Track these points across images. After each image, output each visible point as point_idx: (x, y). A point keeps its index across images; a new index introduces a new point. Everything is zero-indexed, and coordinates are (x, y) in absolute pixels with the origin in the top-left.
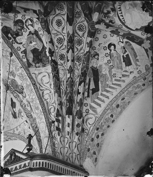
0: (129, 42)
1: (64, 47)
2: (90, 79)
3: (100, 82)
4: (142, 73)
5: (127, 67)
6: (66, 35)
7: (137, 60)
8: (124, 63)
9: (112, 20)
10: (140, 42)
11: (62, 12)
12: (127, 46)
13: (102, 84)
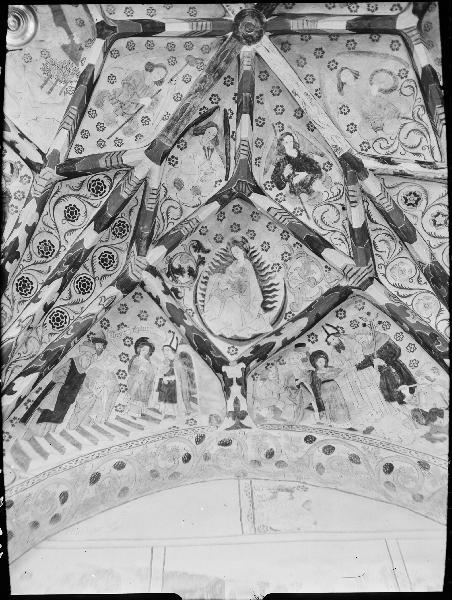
0: (190, 358)
1: (44, 268)
2: (51, 386)
3: (72, 406)
4: (198, 425)
5: (162, 403)
6: (68, 248)
7: (194, 400)
8: (156, 395)
9: (179, 289)
10: (217, 365)
11: (93, 197)
12: (178, 365)
13: (75, 413)
